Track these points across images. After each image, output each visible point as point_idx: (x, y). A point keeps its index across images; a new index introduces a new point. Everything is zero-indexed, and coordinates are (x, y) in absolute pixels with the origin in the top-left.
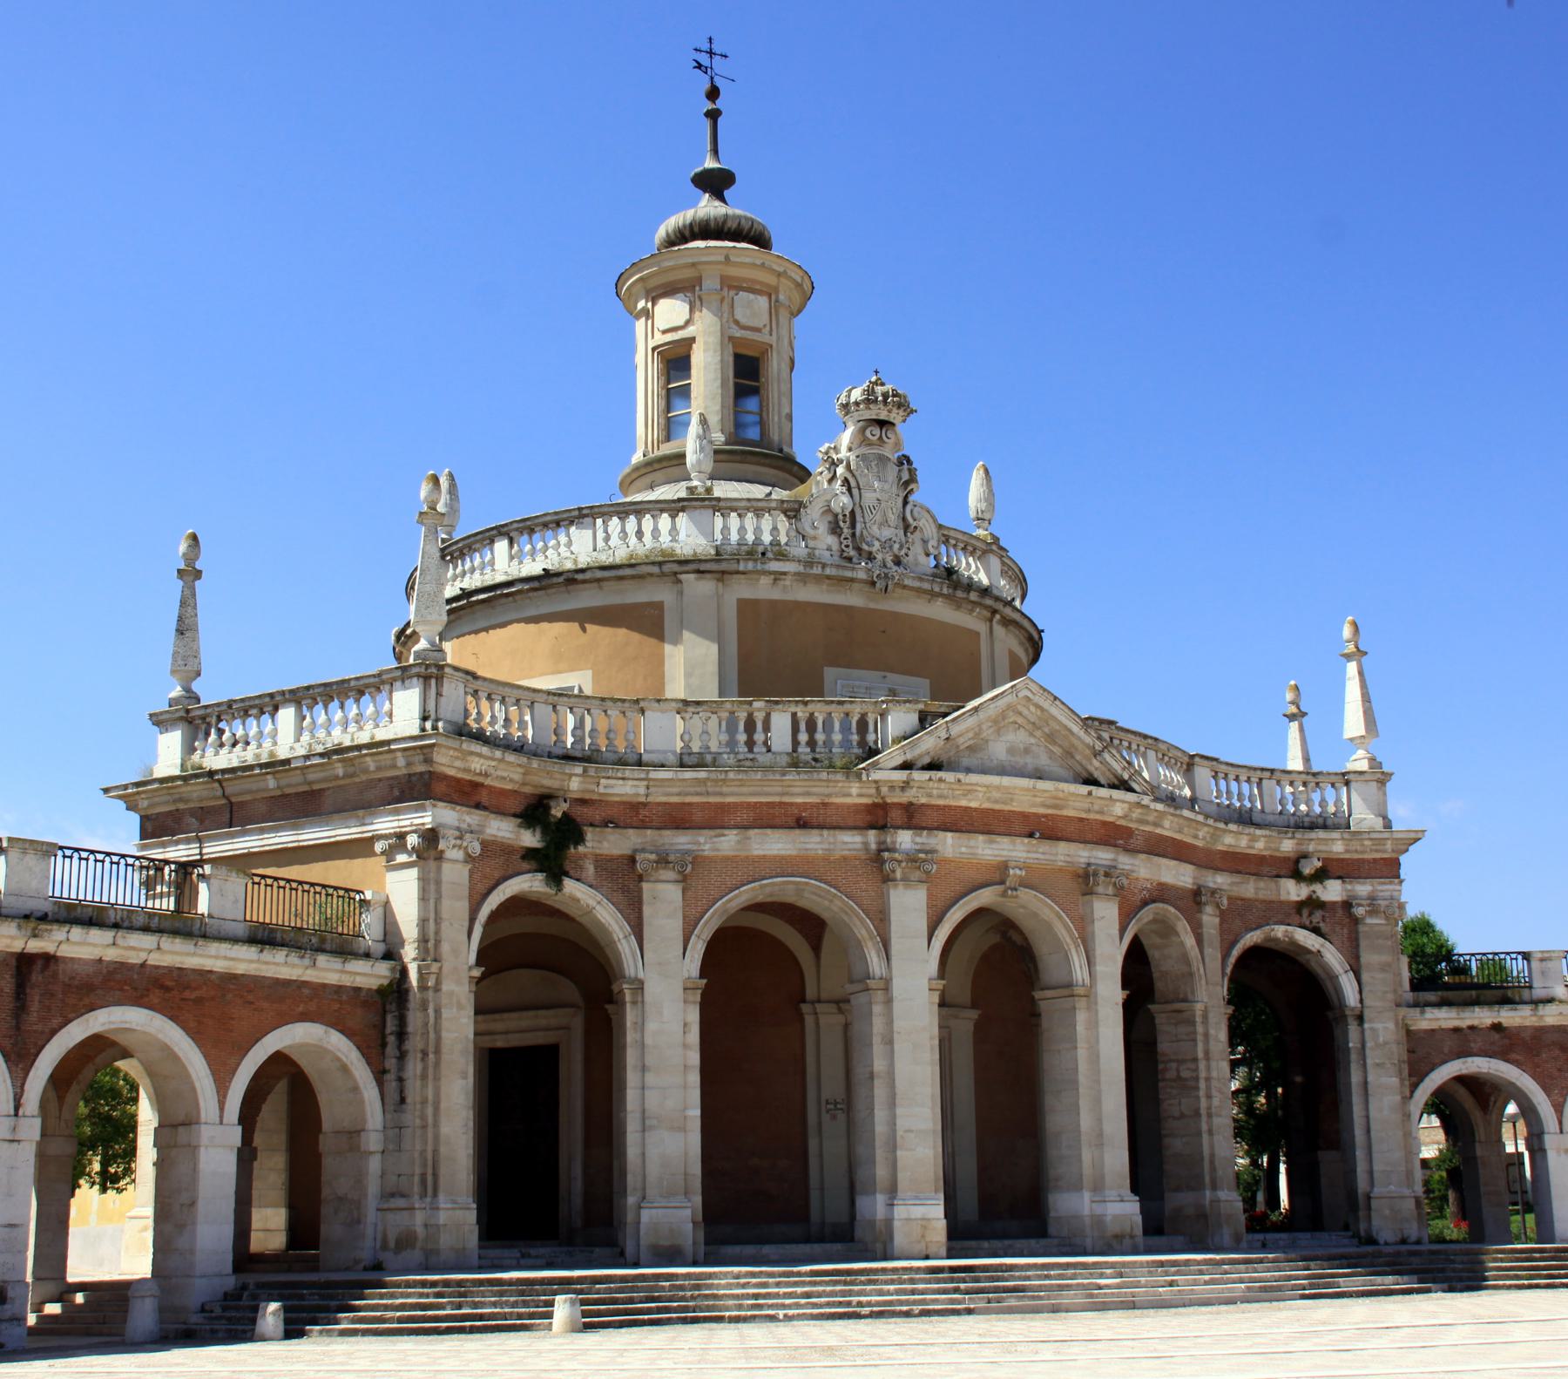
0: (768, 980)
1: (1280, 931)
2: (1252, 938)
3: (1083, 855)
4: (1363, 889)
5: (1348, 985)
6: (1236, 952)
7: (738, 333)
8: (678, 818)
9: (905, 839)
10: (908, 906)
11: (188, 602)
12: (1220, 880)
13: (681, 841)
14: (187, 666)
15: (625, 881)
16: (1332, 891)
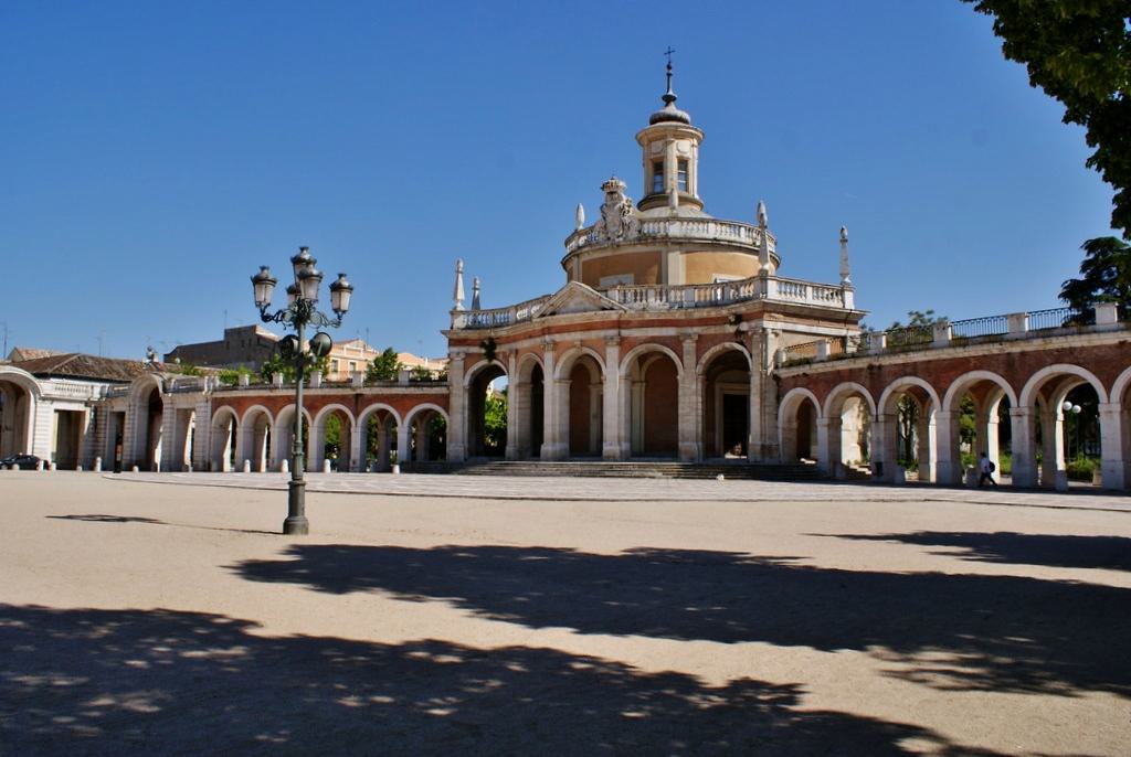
1: (727, 344)
2: (717, 348)
3: (602, 333)
4: (753, 324)
5: (750, 360)
6: (707, 355)
7: (652, 157)
12: (689, 330)
15: (506, 357)
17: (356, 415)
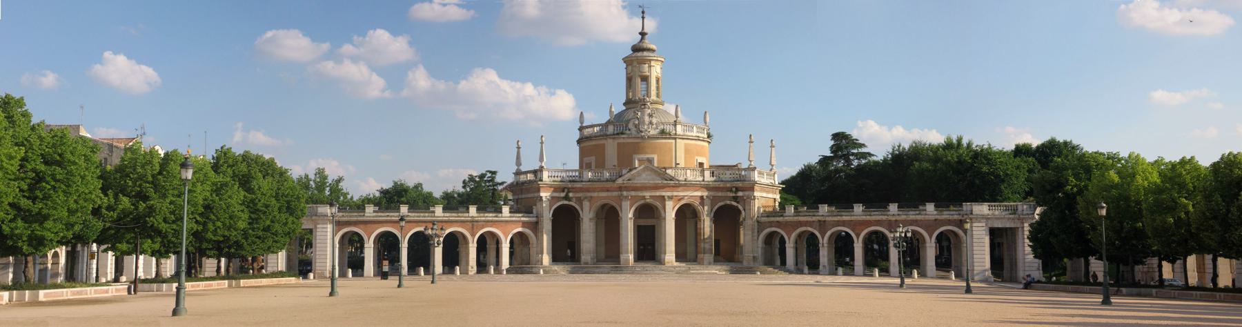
0: (609, 217)
8: (588, 190)
9: (625, 193)
10: (626, 204)
11: (518, 153)
13: (589, 194)
14: (518, 163)
15: (580, 201)
16: (740, 194)
17: (473, 235)
